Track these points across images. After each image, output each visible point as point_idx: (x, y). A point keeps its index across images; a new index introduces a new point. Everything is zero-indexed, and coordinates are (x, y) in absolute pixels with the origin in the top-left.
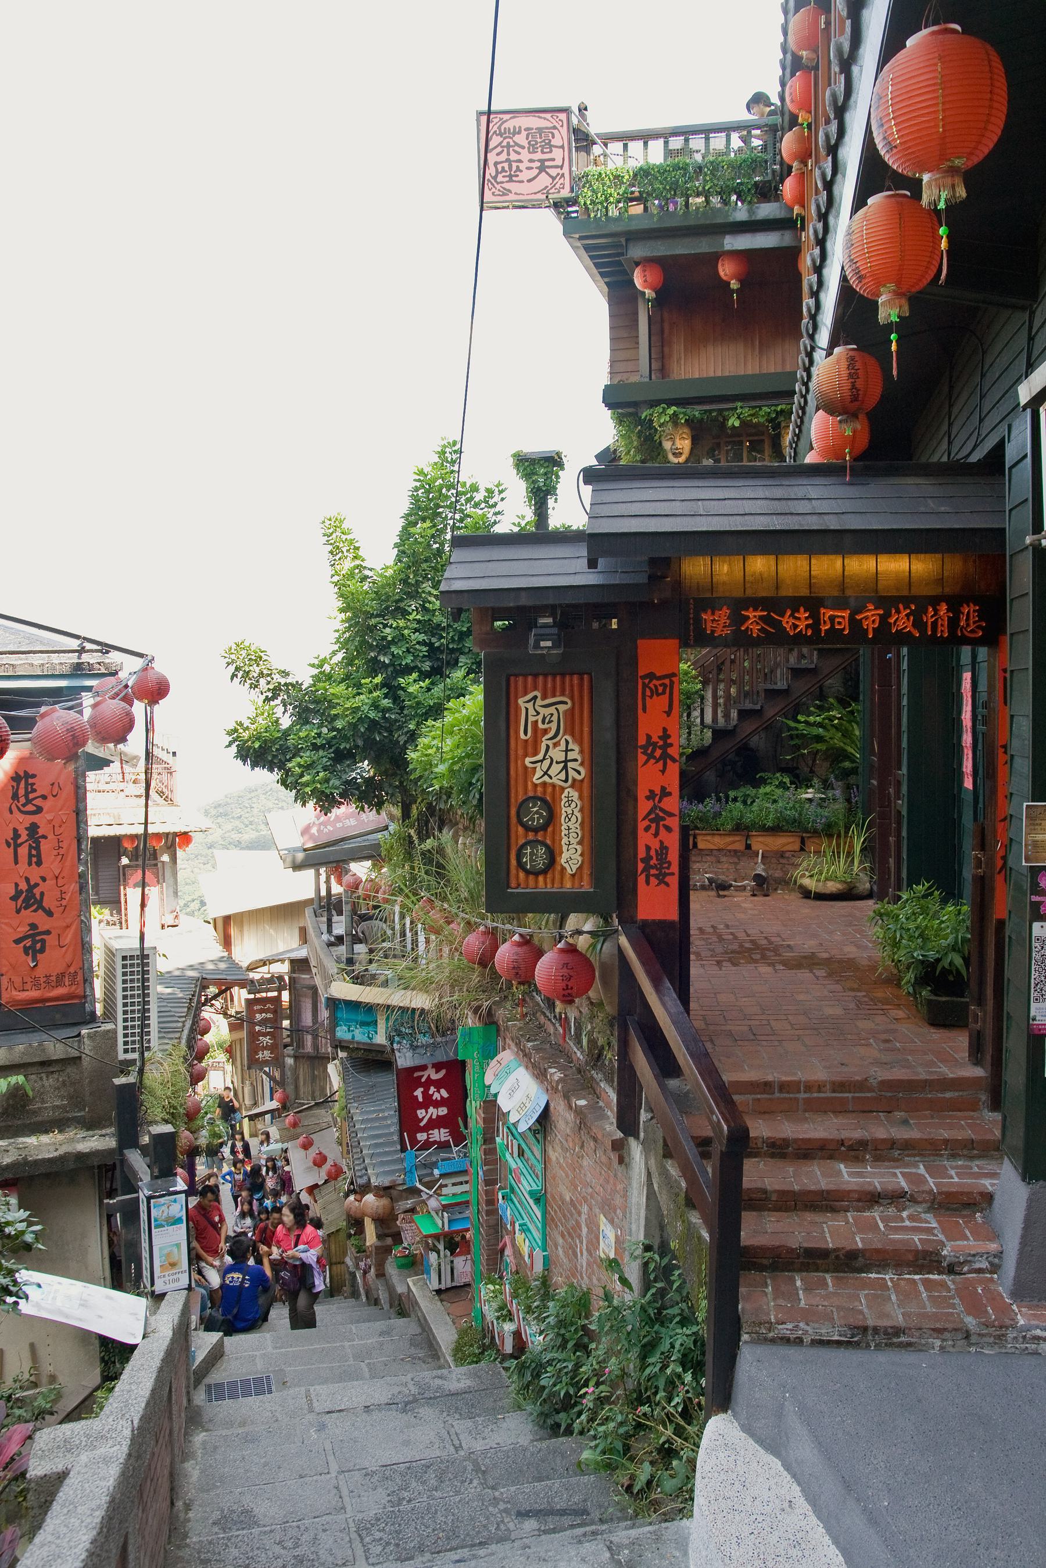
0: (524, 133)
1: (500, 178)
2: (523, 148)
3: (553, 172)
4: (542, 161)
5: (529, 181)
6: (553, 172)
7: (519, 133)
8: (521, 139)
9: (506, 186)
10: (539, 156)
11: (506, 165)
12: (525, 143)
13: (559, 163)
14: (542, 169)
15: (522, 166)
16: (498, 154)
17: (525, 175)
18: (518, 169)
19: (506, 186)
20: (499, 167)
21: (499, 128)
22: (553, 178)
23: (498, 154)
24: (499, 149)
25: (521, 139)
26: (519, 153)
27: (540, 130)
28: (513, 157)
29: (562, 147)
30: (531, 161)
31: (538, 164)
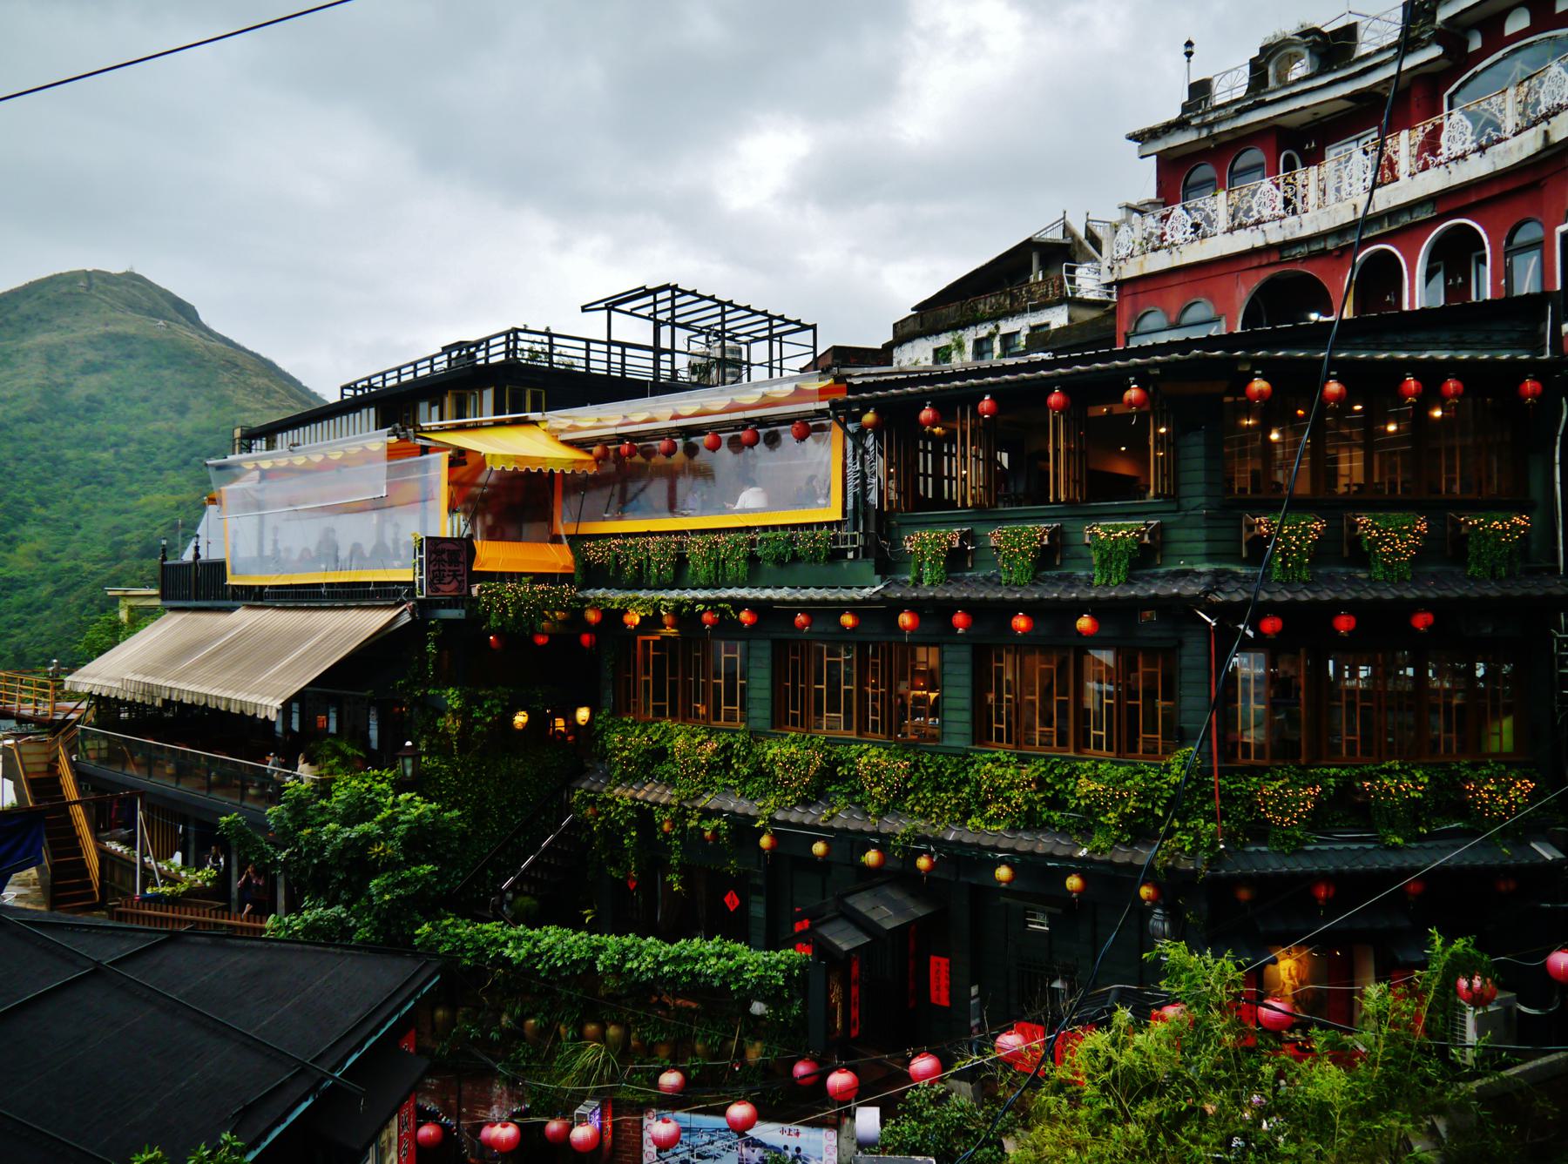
8: (445, 556)
17: (448, 579)
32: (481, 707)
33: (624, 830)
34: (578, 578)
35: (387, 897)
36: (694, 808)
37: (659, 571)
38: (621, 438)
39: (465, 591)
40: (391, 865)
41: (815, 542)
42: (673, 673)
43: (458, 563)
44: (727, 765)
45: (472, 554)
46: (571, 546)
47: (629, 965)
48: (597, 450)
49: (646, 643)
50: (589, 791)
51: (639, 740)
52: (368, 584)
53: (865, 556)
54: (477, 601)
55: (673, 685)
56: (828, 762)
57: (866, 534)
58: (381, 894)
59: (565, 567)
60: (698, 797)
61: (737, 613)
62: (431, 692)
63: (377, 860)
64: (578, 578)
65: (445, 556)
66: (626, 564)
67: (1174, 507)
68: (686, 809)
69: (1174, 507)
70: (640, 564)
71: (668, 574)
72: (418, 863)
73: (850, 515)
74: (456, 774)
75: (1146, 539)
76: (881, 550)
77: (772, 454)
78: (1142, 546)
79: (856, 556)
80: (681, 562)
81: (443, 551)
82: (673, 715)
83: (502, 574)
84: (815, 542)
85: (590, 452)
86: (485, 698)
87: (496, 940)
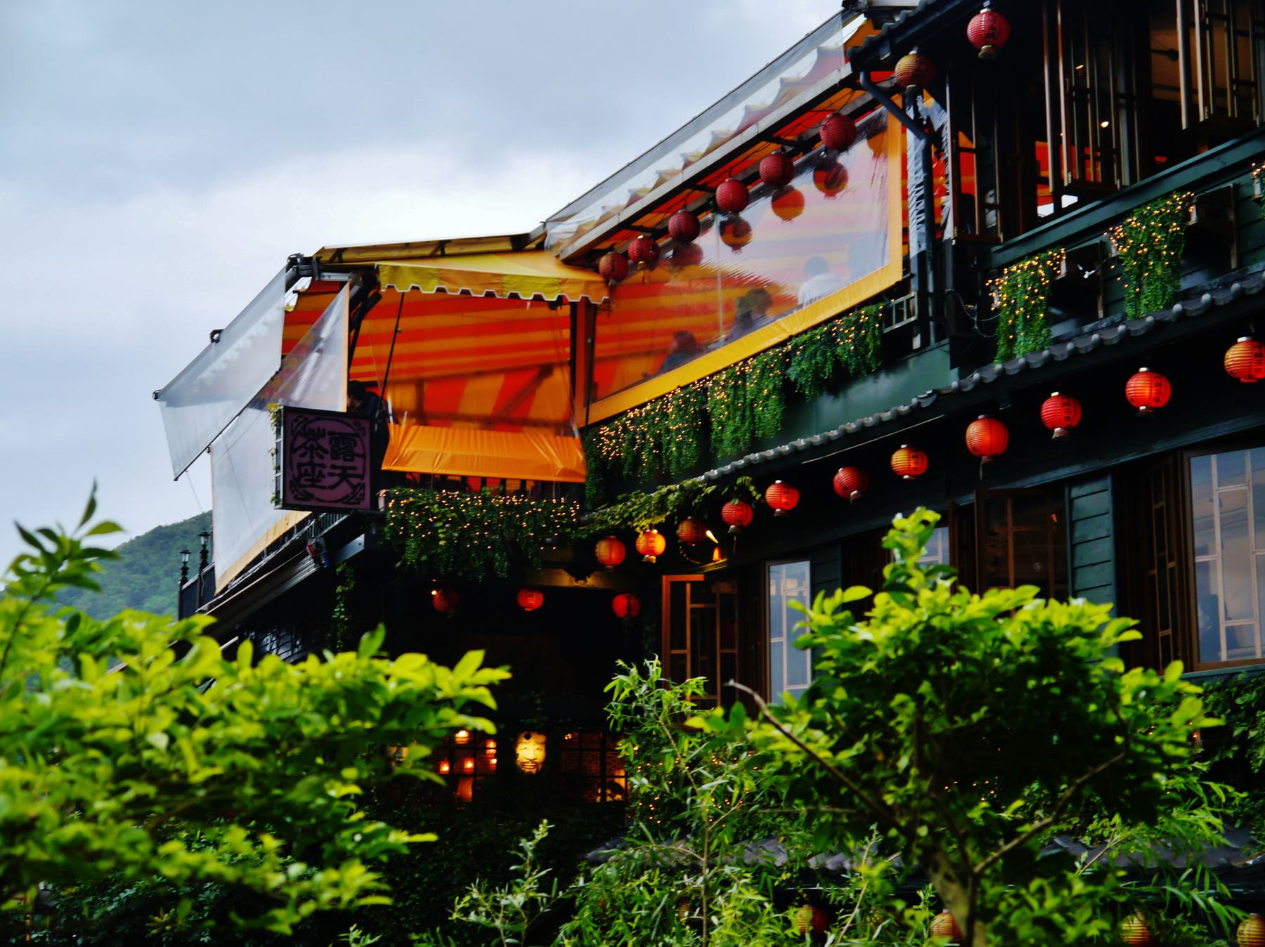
0: (327, 437)
1: (303, 482)
2: (326, 452)
3: (355, 481)
4: (344, 468)
5: (332, 487)
6: (355, 481)
7: (323, 436)
8: (325, 442)
10: (339, 463)
11: (309, 468)
12: (328, 447)
13: (360, 471)
14: (344, 477)
15: (325, 471)
16: (302, 456)
18: (321, 475)
19: (308, 489)
20: (303, 469)
21: (304, 428)
22: (354, 487)
23: (302, 456)
24: (302, 451)
26: (322, 458)
28: (317, 460)
29: (363, 456)
30: (334, 467)
31: (339, 471)
38: (628, 226)
39: (366, 503)
41: (859, 327)
45: (381, 442)
46: (582, 439)
49: (678, 588)
54: (382, 519)
59: (565, 472)
61: (762, 490)
65: (325, 442)
66: (643, 446)
70: (658, 445)
73: (914, 269)
79: (925, 342)
80: (702, 424)
81: (321, 434)
83: (425, 477)
84: (859, 327)
85: (596, 270)
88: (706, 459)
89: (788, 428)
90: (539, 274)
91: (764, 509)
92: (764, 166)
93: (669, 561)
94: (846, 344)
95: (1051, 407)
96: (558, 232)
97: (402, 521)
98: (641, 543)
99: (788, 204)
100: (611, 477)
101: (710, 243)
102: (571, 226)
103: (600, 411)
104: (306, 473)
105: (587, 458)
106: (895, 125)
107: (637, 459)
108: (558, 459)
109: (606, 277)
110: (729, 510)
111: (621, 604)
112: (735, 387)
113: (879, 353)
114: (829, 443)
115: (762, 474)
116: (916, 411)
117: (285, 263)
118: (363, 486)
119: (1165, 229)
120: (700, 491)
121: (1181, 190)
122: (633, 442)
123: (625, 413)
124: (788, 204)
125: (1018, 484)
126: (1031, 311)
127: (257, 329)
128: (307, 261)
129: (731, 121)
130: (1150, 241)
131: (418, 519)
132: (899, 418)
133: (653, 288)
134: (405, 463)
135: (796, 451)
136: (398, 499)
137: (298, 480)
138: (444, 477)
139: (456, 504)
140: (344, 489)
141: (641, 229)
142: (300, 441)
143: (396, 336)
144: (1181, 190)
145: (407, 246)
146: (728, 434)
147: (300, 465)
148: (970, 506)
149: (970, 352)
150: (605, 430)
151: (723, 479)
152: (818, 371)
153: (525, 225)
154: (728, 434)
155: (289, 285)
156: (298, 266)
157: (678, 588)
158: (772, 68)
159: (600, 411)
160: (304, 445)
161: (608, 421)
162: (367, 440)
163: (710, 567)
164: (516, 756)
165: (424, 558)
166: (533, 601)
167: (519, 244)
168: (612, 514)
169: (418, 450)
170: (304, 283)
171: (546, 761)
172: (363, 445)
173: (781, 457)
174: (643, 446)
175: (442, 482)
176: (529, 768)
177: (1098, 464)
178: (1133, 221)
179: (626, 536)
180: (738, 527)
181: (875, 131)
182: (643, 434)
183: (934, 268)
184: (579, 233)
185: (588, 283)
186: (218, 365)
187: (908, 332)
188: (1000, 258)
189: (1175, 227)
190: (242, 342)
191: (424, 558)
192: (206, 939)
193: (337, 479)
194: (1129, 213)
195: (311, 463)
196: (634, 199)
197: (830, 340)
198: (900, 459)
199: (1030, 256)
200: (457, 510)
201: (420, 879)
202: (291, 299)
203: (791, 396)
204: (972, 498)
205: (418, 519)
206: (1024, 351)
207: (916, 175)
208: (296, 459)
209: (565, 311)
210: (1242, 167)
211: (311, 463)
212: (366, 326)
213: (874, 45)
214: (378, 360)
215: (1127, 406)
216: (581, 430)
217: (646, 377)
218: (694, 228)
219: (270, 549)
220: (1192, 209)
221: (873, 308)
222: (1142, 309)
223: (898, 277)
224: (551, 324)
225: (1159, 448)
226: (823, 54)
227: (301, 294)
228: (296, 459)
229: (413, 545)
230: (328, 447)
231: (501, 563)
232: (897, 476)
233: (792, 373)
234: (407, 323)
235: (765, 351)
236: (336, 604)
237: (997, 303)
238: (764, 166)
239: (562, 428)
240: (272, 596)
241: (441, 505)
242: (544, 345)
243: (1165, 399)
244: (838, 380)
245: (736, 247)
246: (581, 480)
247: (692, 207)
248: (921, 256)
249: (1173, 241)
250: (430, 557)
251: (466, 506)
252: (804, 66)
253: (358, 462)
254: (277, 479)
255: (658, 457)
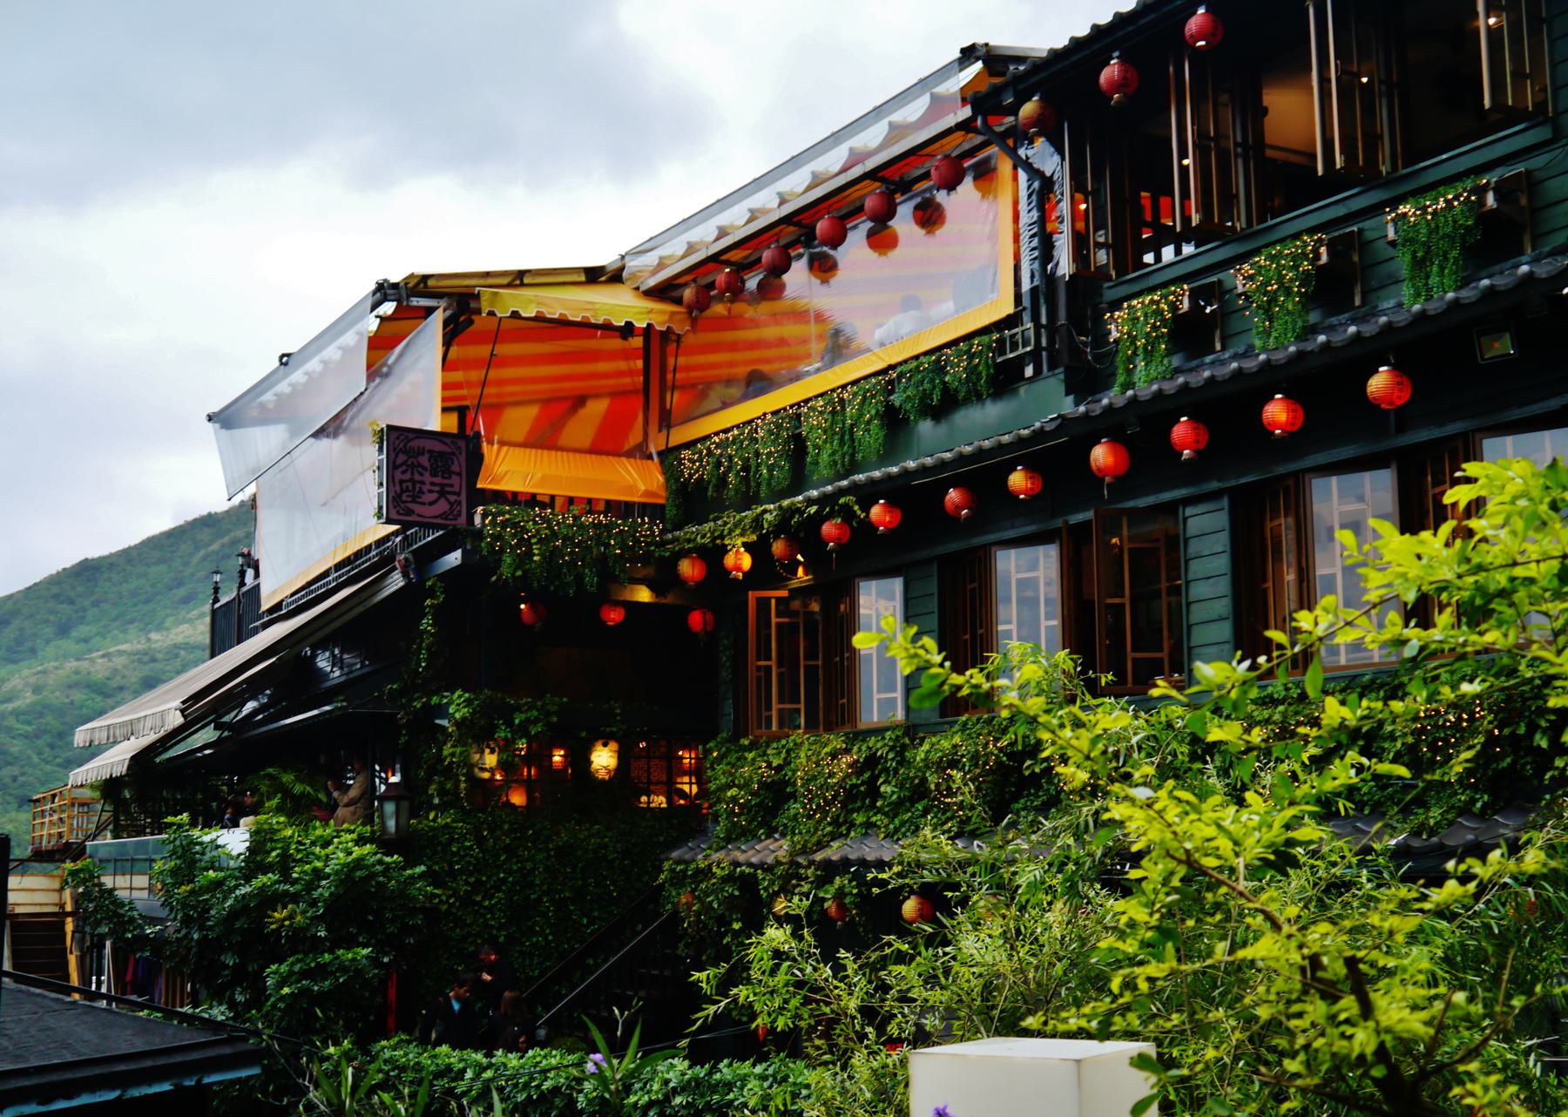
0: (427, 456)
3: (452, 498)
5: (431, 504)
6: (452, 498)
9: (411, 506)
10: (438, 480)
12: (427, 465)
14: (442, 494)
15: (425, 488)
18: (421, 491)
19: (411, 506)
22: (451, 504)
25: (424, 460)
27: (441, 454)
28: (417, 477)
29: (459, 474)
30: (432, 484)
32: (509, 724)
33: (724, 921)
34: (670, 512)
35: (286, 990)
36: (812, 863)
37: (771, 469)
38: (715, 259)
39: (463, 519)
40: (300, 941)
42: (812, 655)
43: (447, 472)
44: (874, 793)
45: (475, 461)
46: (661, 462)
47: (633, 1099)
48: (688, 294)
49: (763, 604)
50: (678, 862)
51: (755, 768)
52: (368, 548)
53: (1052, 367)
54: (479, 535)
55: (811, 672)
56: (1010, 756)
57: (1052, 328)
58: (280, 985)
59: (647, 493)
60: (821, 845)
61: (867, 510)
62: (435, 700)
63: (278, 930)
64: (670, 512)
65: (424, 460)
66: (729, 469)
67: (1543, 133)
68: (799, 865)
69: (1543, 133)
70: (746, 468)
71: (782, 474)
72: (351, 944)
73: (1026, 302)
74: (480, 841)
75: (1490, 199)
76: (1076, 351)
77: (930, 240)
78: (1485, 219)
80: (797, 449)
81: (421, 452)
82: (811, 726)
84: (971, 356)
85: (678, 301)
86: (518, 709)
87: (449, 1068)
88: (798, 481)
89: (889, 452)
90: (620, 305)
91: (869, 526)
92: (869, 203)
93: (755, 578)
94: (956, 373)
95: (1182, 430)
96: (633, 264)
97: (498, 537)
98: (730, 560)
99: (881, 240)
100: (692, 499)
101: (797, 277)
102: (651, 259)
103: (679, 436)
104: (407, 490)
105: (667, 480)
106: (1005, 167)
107: (723, 481)
108: (638, 480)
109: (690, 309)
110: (828, 528)
111: (696, 620)
112: (833, 413)
113: (992, 381)
114: (943, 465)
115: (868, 493)
116: (1039, 435)
117: (373, 287)
118: (460, 503)
119: (1296, 267)
120: (800, 511)
121: (1311, 231)
122: (719, 464)
123: (708, 437)
124: (881, 240)
125: (1131, 504)
126: (1152, 343)
127: (332, 352)
128: (395, 286)
129: (833, 161)
130: (1281, 278)
131: (514, 536)
132: (1021, 442)
133: (731, 322)
134: (498, 482)
135: (906, 473)
136: (495, 516)
137: (400, 496)
138: (534, 495)
139: (548, 521)
140: (442, 506)
141: (728, 263)
142: (402, 458)
143: (491, 362)
144: (1311, 231)
145: (487, 274)
146: (825, 457)
147: (401, 482)
148: (1088, 523)
149: (1084, 382)
150: (686, 453)
151: (823, 500)
152: (926, 396)
153: (603, 257)
154: (825, 457)
155: (374, 308)
156: (384, 291)
157: (763, 604)
158: (878, 112)
159: (679, 436)
160: (404, 463)
161: (690, 445)
162: (463, 458)
163: (794, 584)
164: (590, 763)
165: (519, 573)
166: (614, 616)
167: (593, 276)
168: (700, 532)
169: (511, 469)
170: (388, 308)
171: (617, 769)
172: (460, 464)
173: (889, 478)
174: (729, 469)
175: (532, 500)
176: (602, 775)
177: (1214, 485)
178: (1261, 260)
179: (713, 554)
180: (837, 544)
181: (984, 173)
182: (730, 458)
183: (1047, 302)
184: (661, 265)
185: (673, 313)
186: (283, 387)
187: (1019, 363)
188: (1110, 294)
189: (1306, 266)
190: (314, 365)
191: (519, 573)
192: (322, 934)
193: (436, 495)
194: (1257, 251)
195: (411, 480)
196: (723, 232)
197: (939, 369)
198: (1018, 479)
199: (1152, 290)
200: (549, 527)
201: (504, 879)
202: (373, 324)
203: (895, 423)
204: (1089, 515)
205: (514, 536)
206: (1146, 379)
207: (1028, 216)
208: (398, 476)
209: (637, 342)
210: (1375, 210)
211: (411, 480)
212: (454, 350)
213: (997, 91)
214: (469, 384)
215: (1265, 431)
216: (660, 454)
217: (725, 405)
218: (781, 266)
219: (338, 567)
220: (1323, 250)
221: (985, 339)
222: (1266, 342)
223: (1010, 310)
224: (626, 355)
225: (1281, 470)
226: (935, 99)
227: (383, 319)
228: (398, 476)
229: (509, 560)
230: (427, 465)
231: (591, 579)
232: (1013, 496)
233: (896, 399)
234: (504, 349)
235: (866, 378)
236: (424, 616)
237: (1115, 335)
238: (869, 203)
239: (641, 452)
240: (361, 609)
241: (535, 523)
242: (621, 374)
243: (1299, 424)
244: (943, 406)
245: (825, 281)
246: (662, 501)
247: (783, 242)
248: (1034, 291)
249: (1305, 279)
250: (525, 572)
251: (558, 524)
252: (916, 109)
253: (455, 480)
254: (380, 495)
255: (746, 480)
